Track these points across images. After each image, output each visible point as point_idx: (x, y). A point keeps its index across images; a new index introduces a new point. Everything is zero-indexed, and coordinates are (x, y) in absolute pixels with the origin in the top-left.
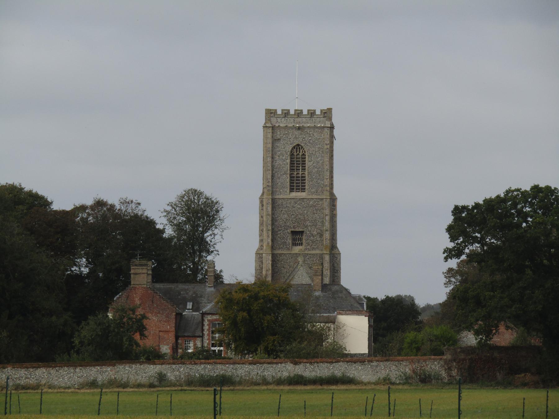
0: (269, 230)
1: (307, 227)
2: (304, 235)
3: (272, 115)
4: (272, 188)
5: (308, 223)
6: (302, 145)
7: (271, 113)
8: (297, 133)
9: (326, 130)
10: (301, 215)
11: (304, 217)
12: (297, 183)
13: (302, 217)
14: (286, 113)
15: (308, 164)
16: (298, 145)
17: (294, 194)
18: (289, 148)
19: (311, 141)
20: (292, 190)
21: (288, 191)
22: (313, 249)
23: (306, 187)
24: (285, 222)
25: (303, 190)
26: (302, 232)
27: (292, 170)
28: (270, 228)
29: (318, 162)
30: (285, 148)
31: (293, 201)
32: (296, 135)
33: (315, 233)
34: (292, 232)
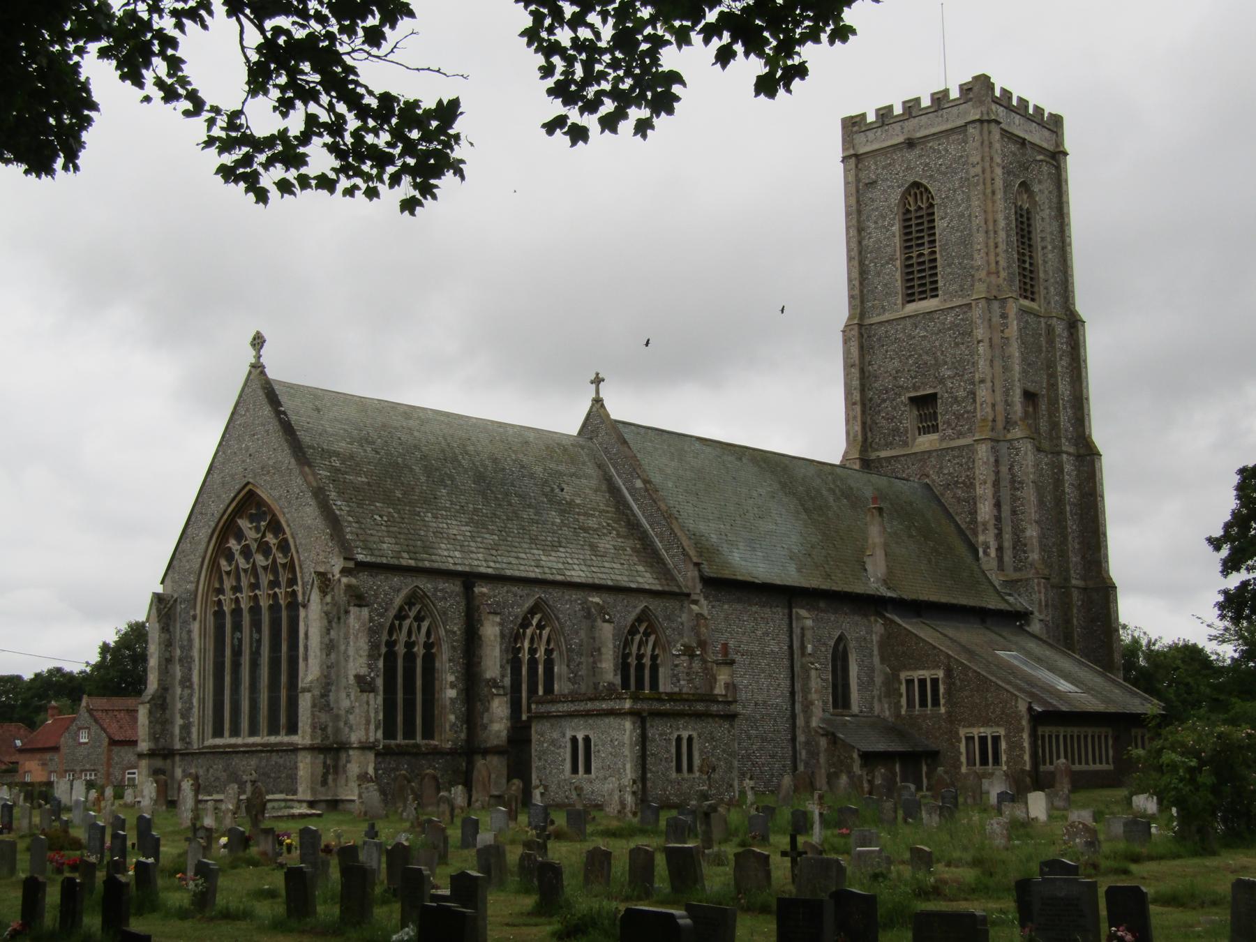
0: (854, 404)
1: (942, 381)
2: (939, 401)
3: (855, 129)
4: (862, 302)
5: (946, 372)
6: (924, 182)
7: (854, 124)
8: (911, 155)
9: (971, 130)
10: (927, 353)
11: (936, 359)
14: (885, 114)
15: (940, 224)
16: (916, 185)
17: (911, 308)
20: (910, 298)
21: (899, 302)
22: (960, 435)
23: (940, 284)
24: (895, 378)
25: (934, 292)
26: (933, 397)
28: (858, 398)
30: (889, 197)
31: (908, 322)
33: (962, 393)
34: (912, 399)
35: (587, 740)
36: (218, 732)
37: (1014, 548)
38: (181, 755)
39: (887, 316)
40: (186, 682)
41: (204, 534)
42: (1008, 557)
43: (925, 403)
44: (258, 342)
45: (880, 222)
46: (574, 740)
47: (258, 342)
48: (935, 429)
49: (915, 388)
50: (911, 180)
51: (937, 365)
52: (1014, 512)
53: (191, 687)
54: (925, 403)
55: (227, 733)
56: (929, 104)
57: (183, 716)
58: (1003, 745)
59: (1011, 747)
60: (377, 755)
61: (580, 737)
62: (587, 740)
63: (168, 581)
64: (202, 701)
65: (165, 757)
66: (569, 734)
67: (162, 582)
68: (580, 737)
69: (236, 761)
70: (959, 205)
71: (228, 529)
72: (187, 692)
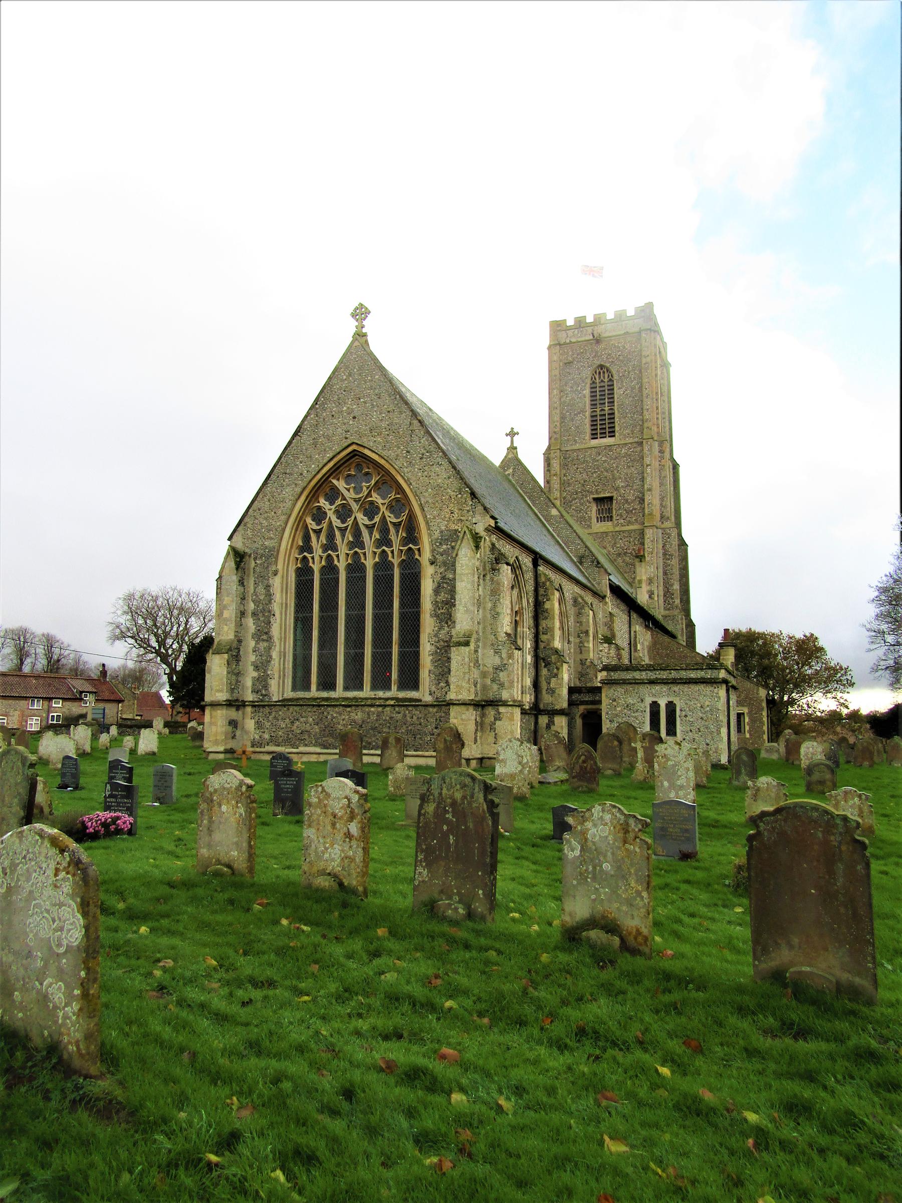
1: (617, 489)
2: (614, 502)
5: (620, 483)
6: (608, 365)
10: (607, 471)
11: (613, 475)
12: (603, 425)
13: (609, 475)
15: (618, 392)
17: (595, 442)
18: (587, 373)
19: (621, 358)
20: (594, 436)
21: (588, 436)
22: (629, 523)
23: (617, 429)
24: (583, 485)
25: (612, 434)
26: (611, 499)
27: (593, 405)
29: (633, 388)
31: (594, 451)
32: (597, 352)
33: (631, 498)
34: (594, 499)
35: (671, 707)
36: (381, 681)
37: (665, 596)
38: (254, 706)
39: (577, 446)
40: (263, 634)
41: (289, 492)
42: (662, 599)
43: (604, 502)
44: (360, 313)
45: (575, 388)
46: (655, 706)
47: (360, 313)
48: (610, 518)
49: (597, 492)
50: (598, 363)
51: (614, 479)
52: (665, 573)
53: (270, 639)
54: (604, 502)
55: (314, 687)
56: (613, 317)
57: (257, 668)
58: (747, 720)
59: (753, 721)
60: (524, 712)
61: (663, 703)
62: (671, 707)
63: (238, 538)
64: (283, 654)
65: (238, 708)
66: (649, 700)
67: (230, 539)
68: (663, 703)
69: (333, 712)
70: (632, 381)
71: (323, 488)
72: (263, 645)
